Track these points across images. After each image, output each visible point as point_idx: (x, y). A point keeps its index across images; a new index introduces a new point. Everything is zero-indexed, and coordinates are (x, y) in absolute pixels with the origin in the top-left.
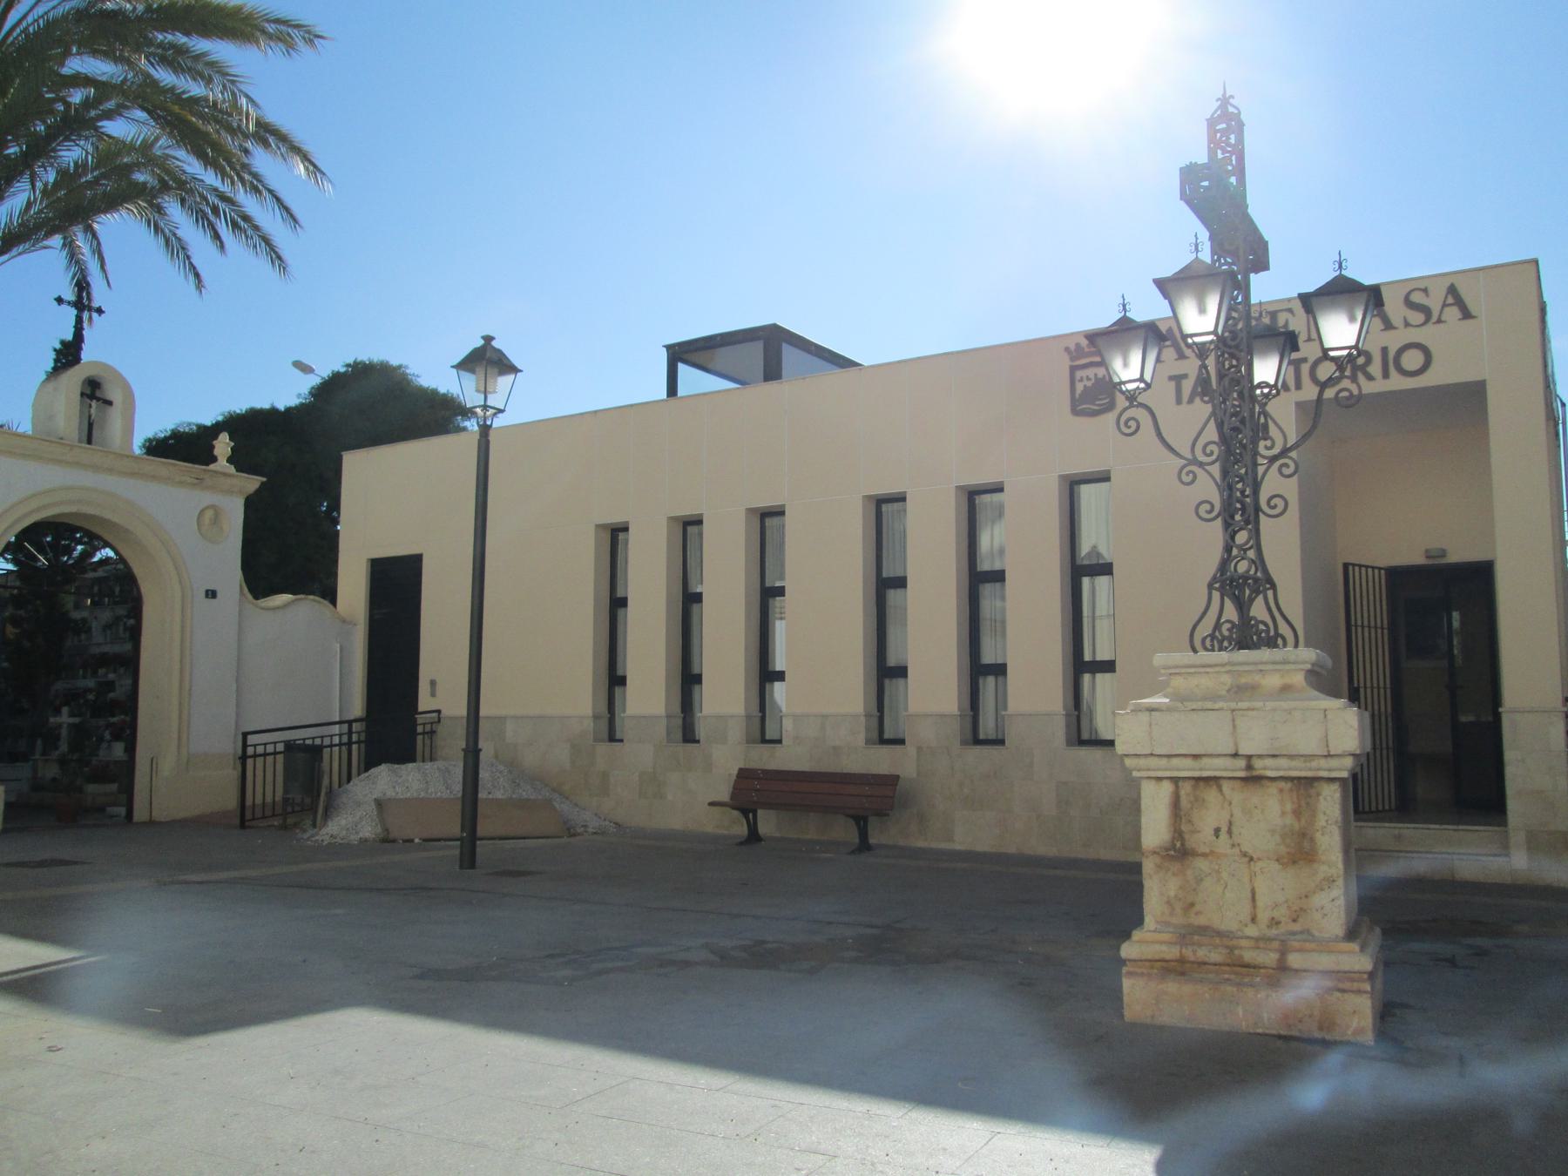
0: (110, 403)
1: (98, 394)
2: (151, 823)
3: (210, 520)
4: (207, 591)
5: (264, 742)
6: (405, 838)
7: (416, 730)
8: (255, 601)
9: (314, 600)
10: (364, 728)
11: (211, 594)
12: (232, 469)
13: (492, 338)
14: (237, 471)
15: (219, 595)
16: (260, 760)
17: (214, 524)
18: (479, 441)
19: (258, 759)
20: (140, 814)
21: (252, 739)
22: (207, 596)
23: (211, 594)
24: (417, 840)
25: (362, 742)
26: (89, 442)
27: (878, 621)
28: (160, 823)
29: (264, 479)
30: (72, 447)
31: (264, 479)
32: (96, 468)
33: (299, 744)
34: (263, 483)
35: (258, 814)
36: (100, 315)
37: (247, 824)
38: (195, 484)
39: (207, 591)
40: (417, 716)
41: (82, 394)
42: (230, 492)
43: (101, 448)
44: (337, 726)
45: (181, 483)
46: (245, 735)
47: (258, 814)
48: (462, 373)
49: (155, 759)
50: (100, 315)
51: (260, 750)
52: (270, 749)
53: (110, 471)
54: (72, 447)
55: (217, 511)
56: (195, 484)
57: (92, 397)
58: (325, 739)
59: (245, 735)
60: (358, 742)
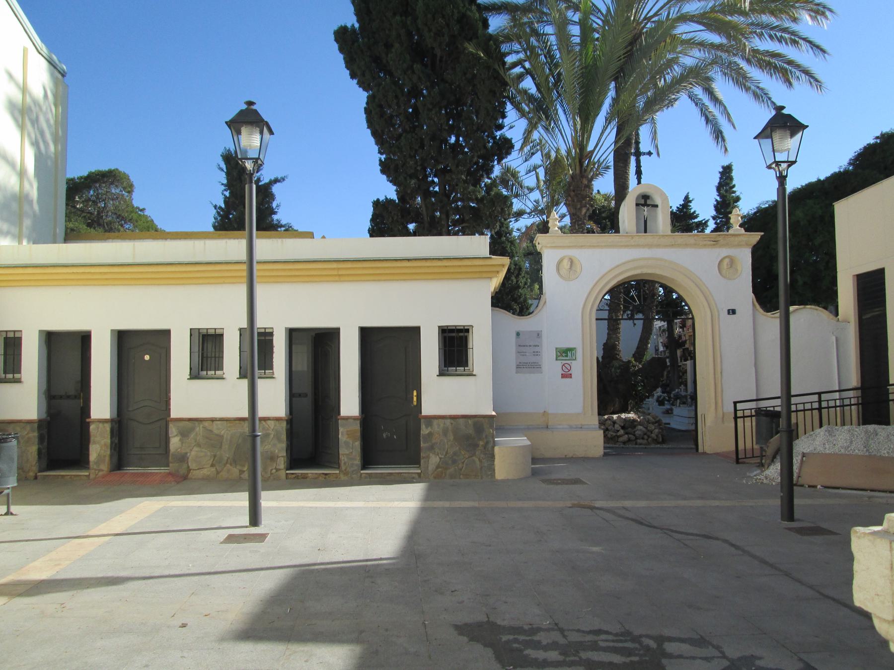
0: (657, 206)
1: (649, 202)
2: (704, 453)
3: (727, 266)
4: (729, 311)
5: (796, 403)
6: (811, 484)
7: (889, 397)
8: (765, 313)
9: (811, 308)
10: (860, 395)
11: (732, 312)
12: (742, 231)
13: (783, 108)
14: (745, 232)
15: (737, 312)
16: (801, 414)
17: (731, 267)
18: (778, 189)
19: (799, 413)
20: (700, 449)
21: (739, 406)
22: (729, 313)
23: (732, 312)
24: (819, 487)
25: (754, 416)
26: (646, 231)
27: (789, 330)
28: (708, 454)
29: (763, 233)
30: (632, 237)
31: (763, 233)
32: (650, 246)
33: (769, 410)
34: (762, 236)
35: (749, 455)
36: (650, 156)
37: (740, 461)
38: (714, 245)
39: (729, 311)
40: (888, 387)
41: (637, 205)
42: (739, 245)
43: (655, 234)
44: (838, 393)
45: (705, 245)
46: (735, 403)
47: (749, 455)
48: (762, 141)
49: (703, 416)
50: (650, 156)
51: (800, 407)
52: (808, 406)
53: (658, 246)
54: (632, 237)
55: (732, 261)
56: (714, 245)
57: (645, 205)
58: (852, 399)
59: (735, 403)
60: (857, 404)
